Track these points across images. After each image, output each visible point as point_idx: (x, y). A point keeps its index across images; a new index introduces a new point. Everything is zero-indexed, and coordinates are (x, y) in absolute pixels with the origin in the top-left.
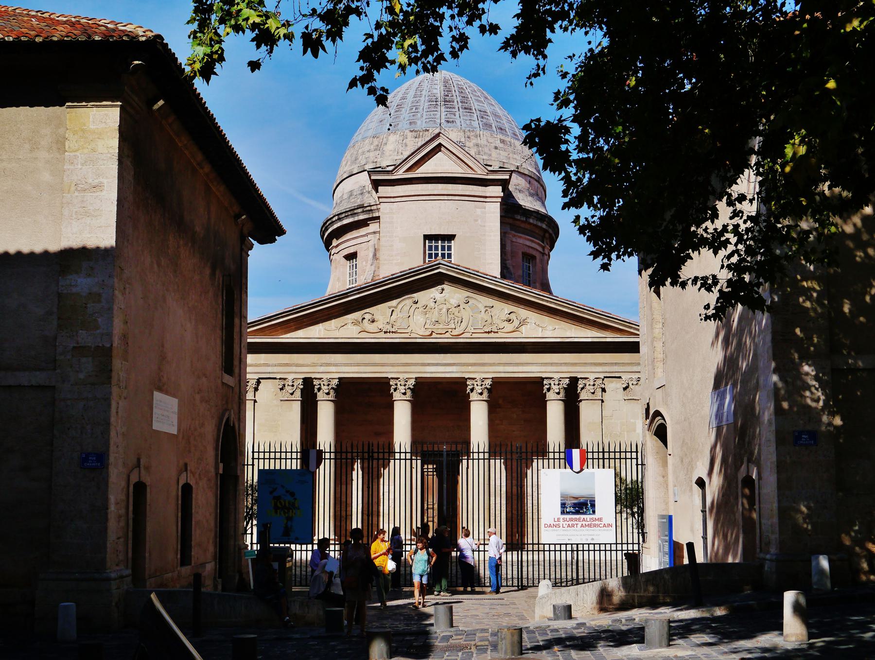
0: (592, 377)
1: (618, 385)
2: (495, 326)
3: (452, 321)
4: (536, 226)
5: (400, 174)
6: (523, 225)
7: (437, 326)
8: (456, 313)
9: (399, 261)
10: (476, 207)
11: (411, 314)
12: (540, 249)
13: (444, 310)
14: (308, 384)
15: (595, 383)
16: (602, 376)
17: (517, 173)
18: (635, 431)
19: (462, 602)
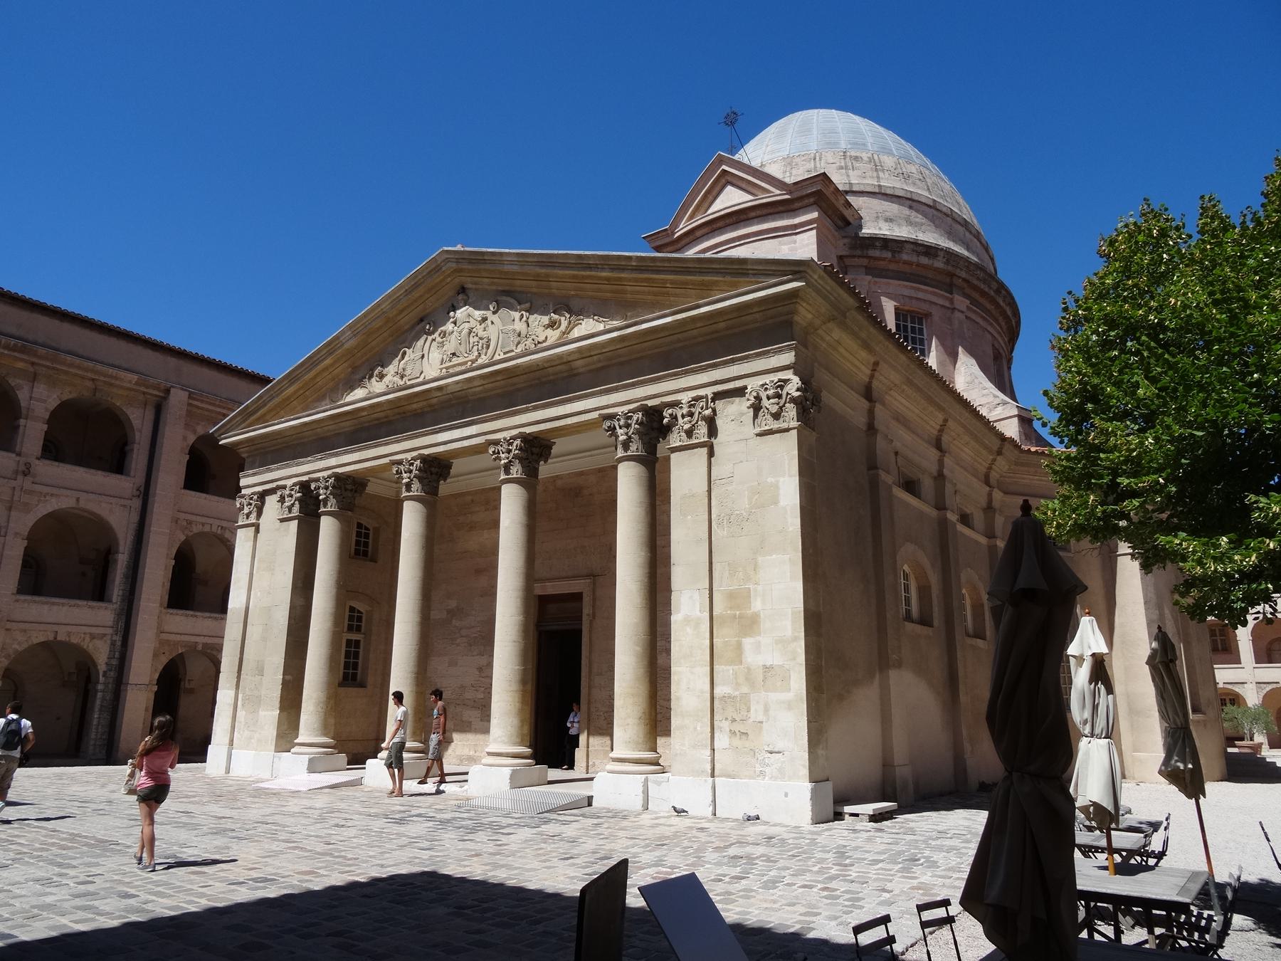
0: (685, 397)
1: (739, 407)
2: (530, 340)
3: (476, 348)
4: (924, 266)
6: (892, 267)
7: (455, 361)
8: (481, 333)
10: (780, 244)
11: (426, 352)
12: (947, 304)
13: (465, 331)
14: (304, 486)
15: (693, 410)
16: (709, 391)
17: (880, 196)
18: (776, 503)
19: (1168, 838)
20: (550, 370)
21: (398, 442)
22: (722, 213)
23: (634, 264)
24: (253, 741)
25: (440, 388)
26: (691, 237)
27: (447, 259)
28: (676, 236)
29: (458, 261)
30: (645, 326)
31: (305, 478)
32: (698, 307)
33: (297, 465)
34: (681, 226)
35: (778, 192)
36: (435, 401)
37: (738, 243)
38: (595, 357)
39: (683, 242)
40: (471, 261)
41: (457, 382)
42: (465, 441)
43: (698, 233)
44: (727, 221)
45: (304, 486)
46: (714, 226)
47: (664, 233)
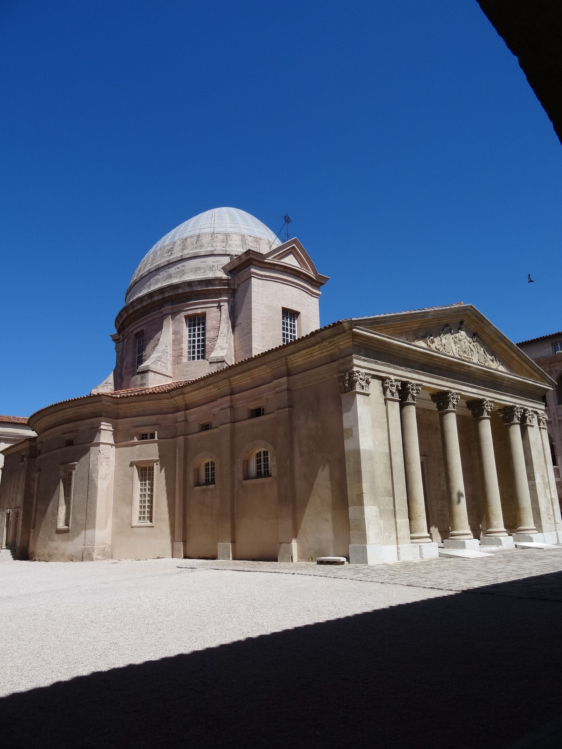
5: (269, 260)
9: (265, 322)
20: (499, 380)
21: (447, 381)
22: (294, 268)
23: (524, 358)
24: (391, 539)
25: (469, 366)
26: (272, 267)
27: (470, 309)
28: (266, 261)
29: (472, 313)
30: (527, 381)
31: (405, 380)
32: (537, 383)
33: (395, 368)
34: (270, 258)
35: (313, 274)
36: (462, 370)
37: (295, 286)
38: (510, 383)
39: (266, 266)
40: (477, 317)
41: (475, 368)
42: (472, 394)
43: (277, 268)
44: (293, 272)
45: (404, 384)
46: (286, 270)
47: (260, 255)
